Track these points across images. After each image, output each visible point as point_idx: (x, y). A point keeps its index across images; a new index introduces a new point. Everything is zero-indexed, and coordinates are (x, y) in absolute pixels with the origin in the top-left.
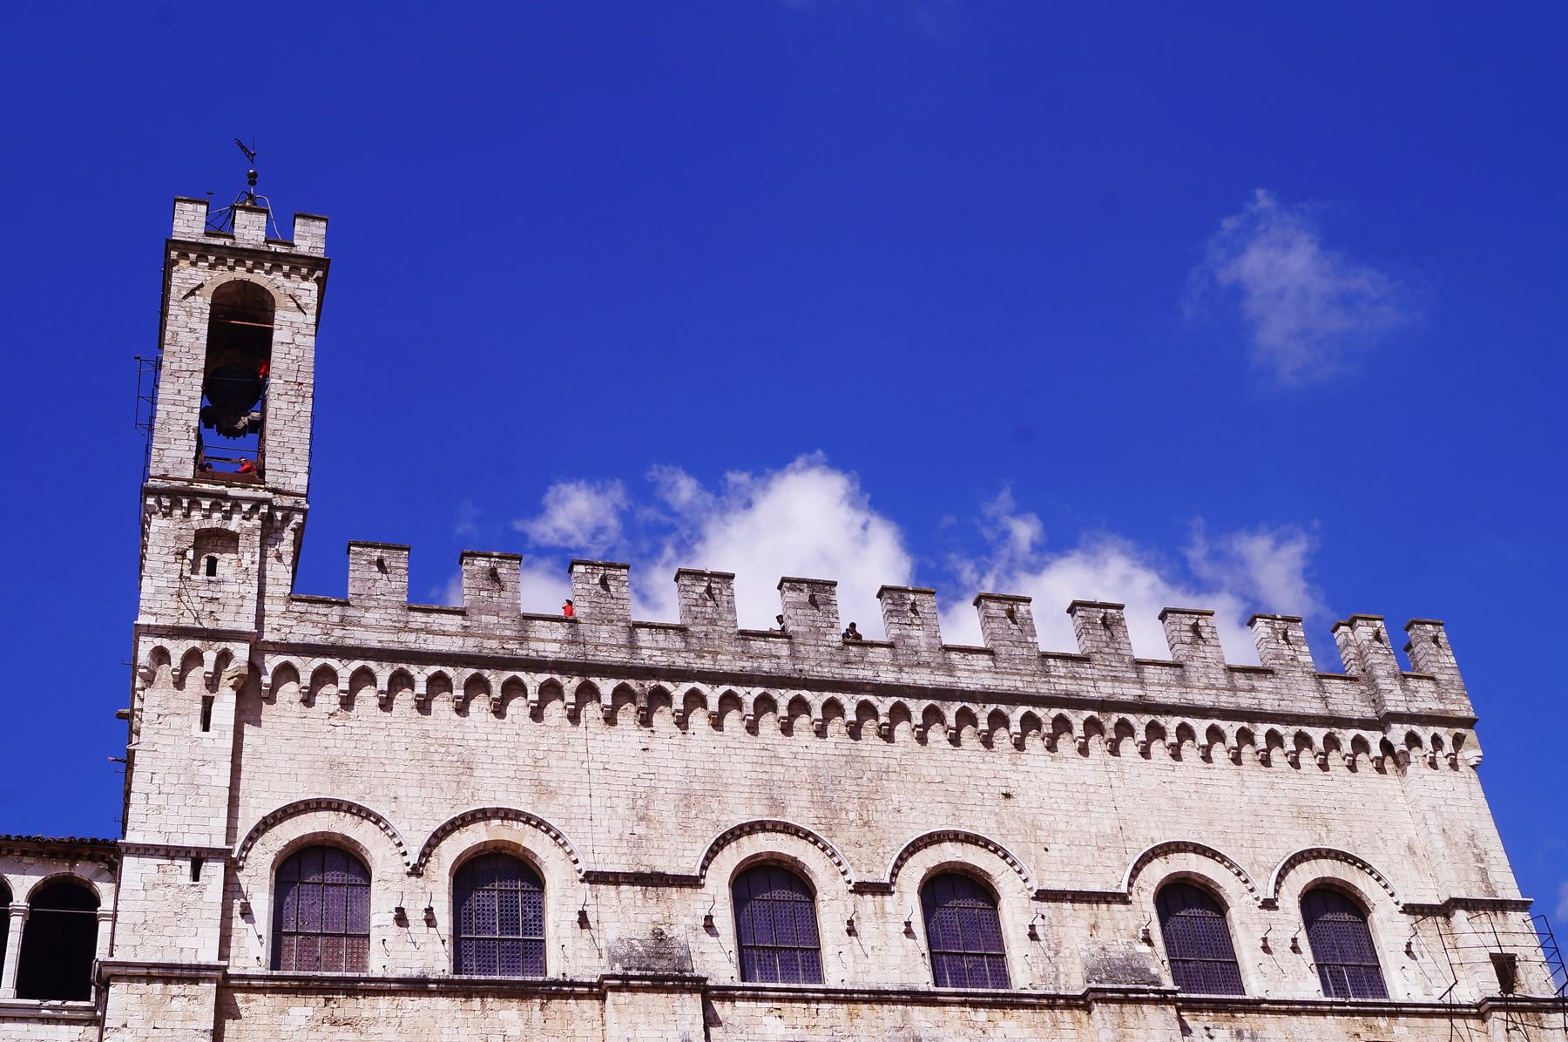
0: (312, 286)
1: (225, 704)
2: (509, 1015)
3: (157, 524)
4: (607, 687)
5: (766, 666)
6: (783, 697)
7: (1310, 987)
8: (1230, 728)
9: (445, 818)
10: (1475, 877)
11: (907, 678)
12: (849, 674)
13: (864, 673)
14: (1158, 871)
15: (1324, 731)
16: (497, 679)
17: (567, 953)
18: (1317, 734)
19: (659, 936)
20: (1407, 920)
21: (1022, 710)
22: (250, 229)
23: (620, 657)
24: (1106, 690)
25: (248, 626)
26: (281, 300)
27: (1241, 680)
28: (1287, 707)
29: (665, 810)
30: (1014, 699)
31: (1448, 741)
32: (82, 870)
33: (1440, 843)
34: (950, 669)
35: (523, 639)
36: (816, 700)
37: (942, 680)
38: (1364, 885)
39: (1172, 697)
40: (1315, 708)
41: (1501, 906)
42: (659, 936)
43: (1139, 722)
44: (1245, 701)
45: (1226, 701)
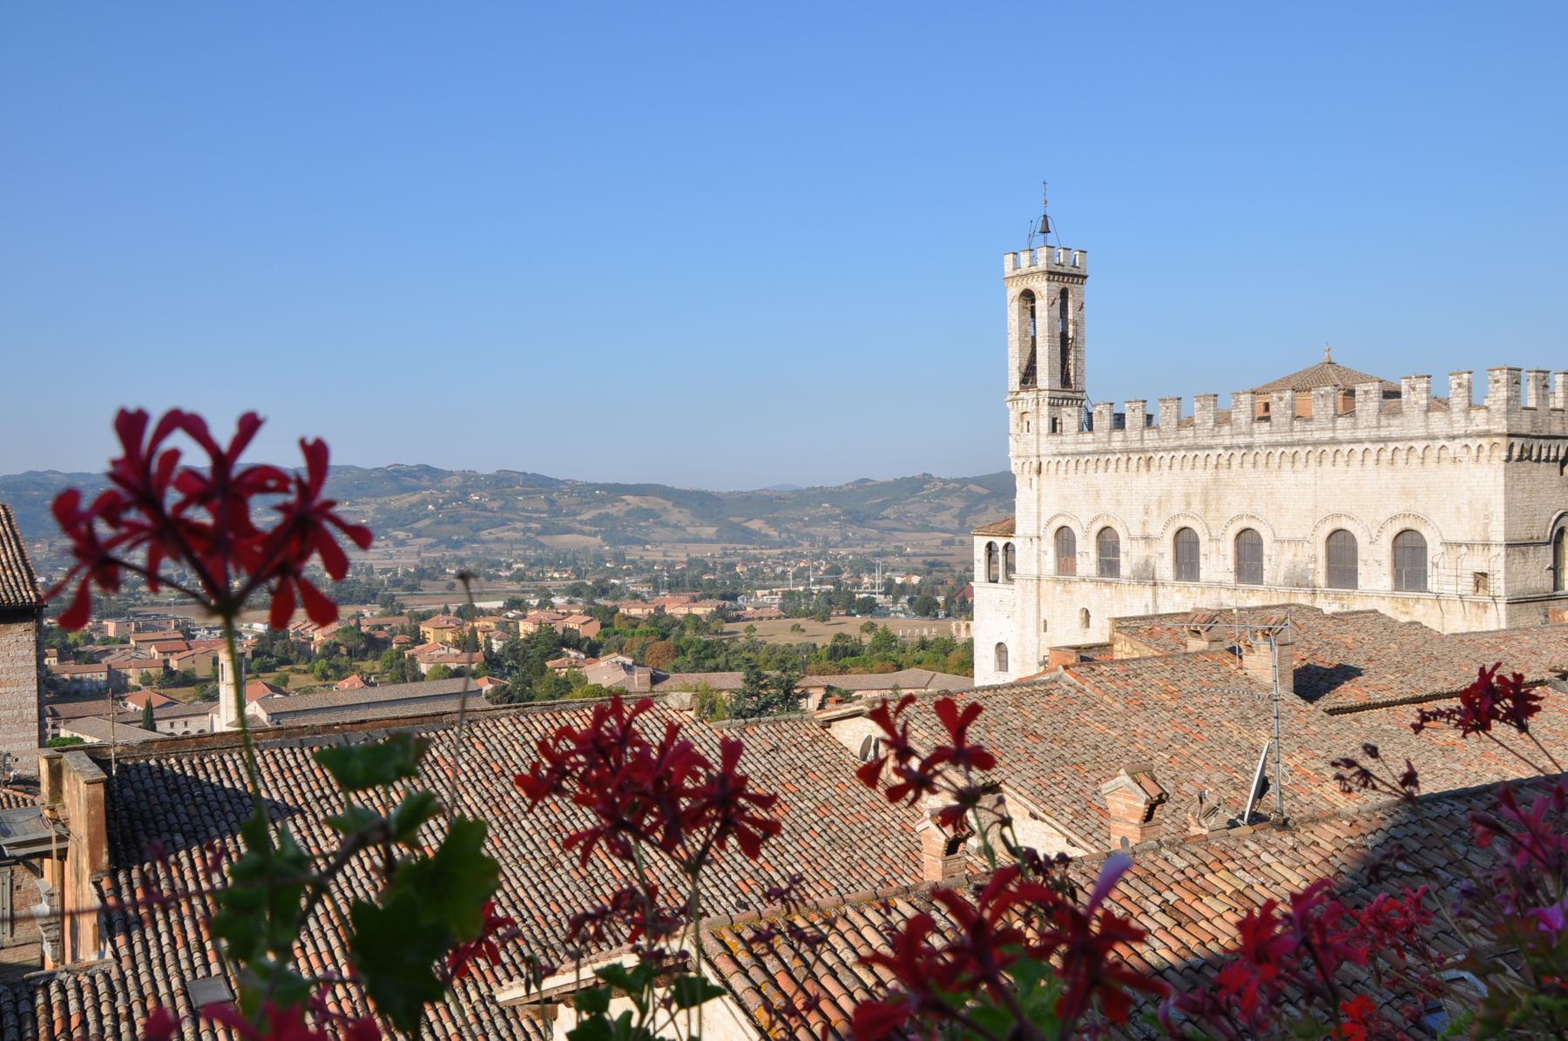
0: (1045, 284)
1: (1035, 477)
2: (1107, 591)
3: (1012, 413)
4: (1134, 457)
5: (1185, 442)
6: (1191, 455)
7: (1387, 582)
8: (1374, 448)
9: (1093, 516)
10: (1479, 528)
11: (1234, 441)
12: (1213, 442)
13: (1219, 441)
14: (1328, 528)
15: (1425, 444)
16: (1103, 458)
17: (1125, 568)
18: (1419, 446)
19: (1147, 563)
20: (1442, 549)
21: (1281, 450)
22: (1024, 258)
23: (1138, 445)
24: (1317, 435)
25: (1034, 452)
26: (1037, 296)
27: (1384, 422)
28: (1405, 433)
29: (1154, 508)
30: (1276, 445)
31: (1487, 447)
32: (1011, 540)
33: (1465, 509)
34: (1251, 434)
35: (1109, 441)
36: (1202, 454)
37: (1248, 440)
38: (1427, 533)
39: (1348, 435)
40: (1422, 432)
41: (1486, 545)
42: (1147, 563)
43: (1330, 450)
44: (1383, 433)
45: (1374, 433)
